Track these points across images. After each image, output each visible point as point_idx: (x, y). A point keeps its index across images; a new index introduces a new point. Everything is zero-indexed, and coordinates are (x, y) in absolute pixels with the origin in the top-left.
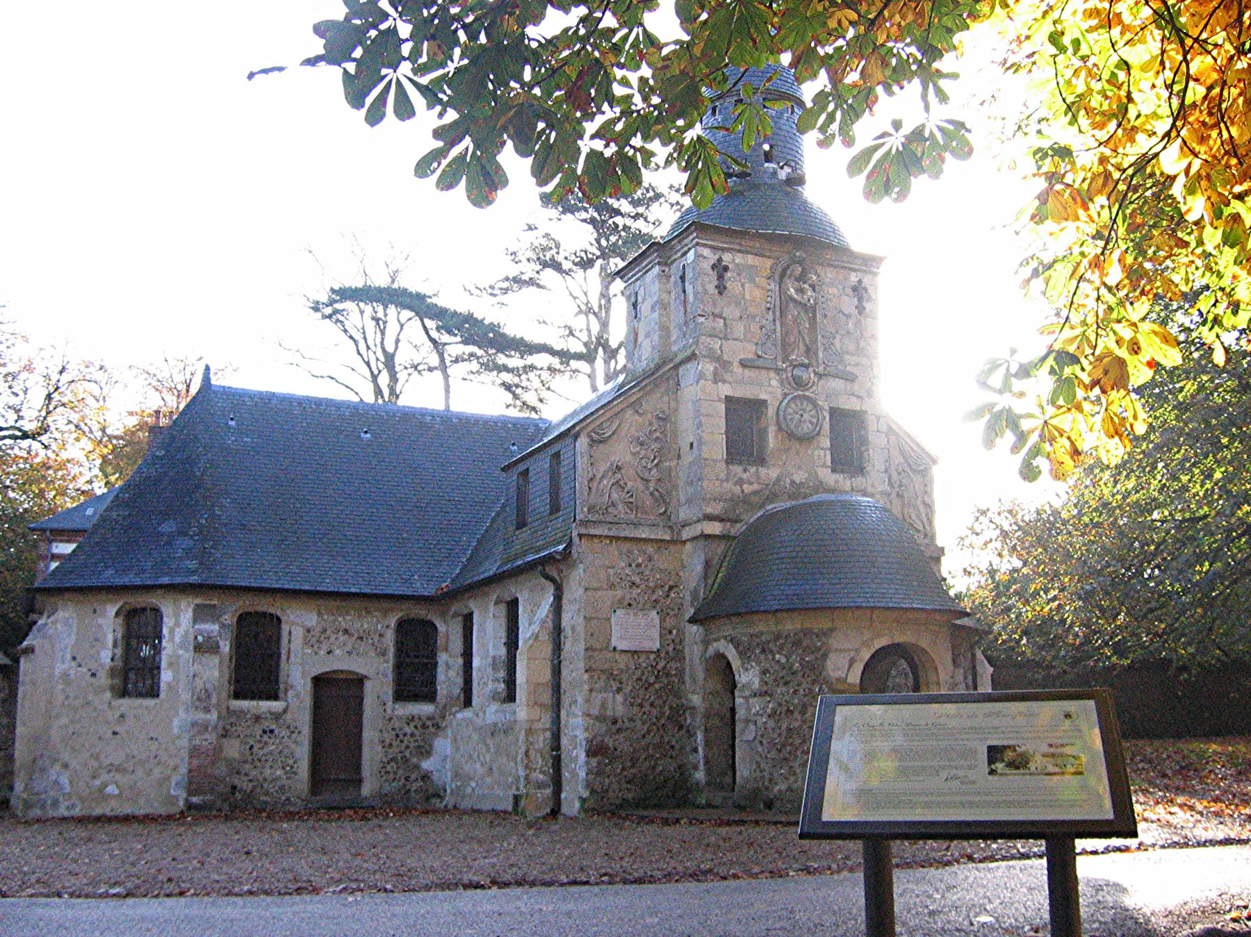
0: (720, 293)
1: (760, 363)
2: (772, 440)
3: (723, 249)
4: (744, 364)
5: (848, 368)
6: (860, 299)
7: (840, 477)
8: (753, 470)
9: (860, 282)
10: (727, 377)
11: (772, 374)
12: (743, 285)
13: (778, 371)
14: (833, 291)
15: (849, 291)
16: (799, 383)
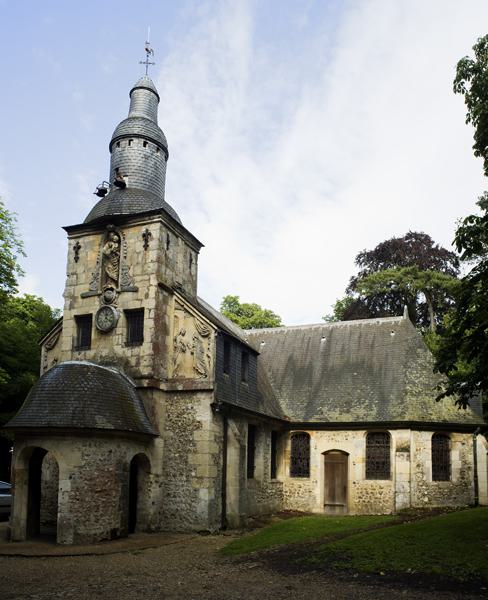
2: (93, 336)
4: (84, 297)
5: (136, 285)
6: (146, 241)
7: (125, 349)
8: (83, 353)
9: (147, 230)
10: (76, 306)
11: (96, 298)
13: (99, 295)
14: (132, 241)
15: (141, 238)
16: (108, 301)
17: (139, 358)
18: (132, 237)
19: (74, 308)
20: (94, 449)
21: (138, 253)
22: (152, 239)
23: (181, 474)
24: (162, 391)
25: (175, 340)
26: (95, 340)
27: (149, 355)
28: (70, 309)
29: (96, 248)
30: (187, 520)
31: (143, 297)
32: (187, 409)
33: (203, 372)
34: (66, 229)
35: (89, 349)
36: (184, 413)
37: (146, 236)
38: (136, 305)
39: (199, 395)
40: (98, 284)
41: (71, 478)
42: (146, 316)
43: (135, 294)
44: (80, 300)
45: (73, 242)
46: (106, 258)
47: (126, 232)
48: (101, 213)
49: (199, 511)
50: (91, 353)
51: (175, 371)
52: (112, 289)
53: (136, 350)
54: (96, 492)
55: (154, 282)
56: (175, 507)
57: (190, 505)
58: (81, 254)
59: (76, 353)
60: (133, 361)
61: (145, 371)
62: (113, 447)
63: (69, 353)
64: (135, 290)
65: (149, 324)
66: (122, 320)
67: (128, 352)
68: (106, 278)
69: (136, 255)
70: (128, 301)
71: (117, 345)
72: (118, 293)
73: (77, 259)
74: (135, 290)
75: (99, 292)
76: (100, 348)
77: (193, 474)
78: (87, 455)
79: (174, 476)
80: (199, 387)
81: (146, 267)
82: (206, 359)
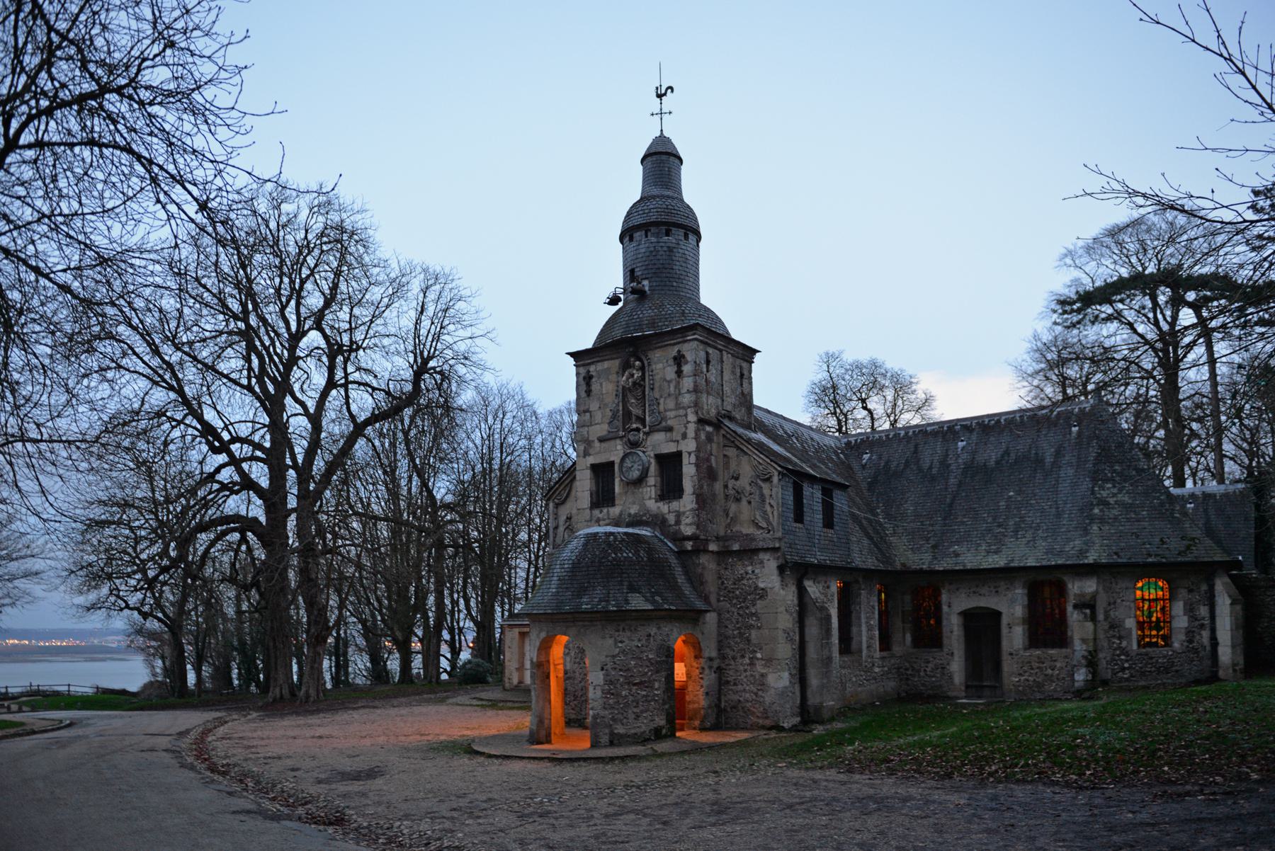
0: (589, 395)
1: (611, 435)
2: (617, 488)
3: (589, 364)
4: (601, 440)
7: (660, 504)
8: (605, 510)
9: (679, 351)
11: (618, 441)
12: (601, 384)
13: (621, 438)
14: (660, 366)
15: (671, 362)
17: (679, 515)
18: (661, 364)
19: (590, 455)
20: (628, 634)
21: (669, 382)
22: (687, 362)
23: (743, 657)
24: (712, 552)
25: (726, 486)
26: (620, 494)
27: (692, 510)
28: (584, 457)
29: (613, 377)
30: (753, 713)
31: (679, 438)
32: (747, 573)
33: (765, 525)
34: (572, 354)
35: (613, 505)
36: (743, 578)
37: (679, 360)
38: (670, 448)
39: (762, 556)
40: (620, 424)
41: (602, 669)
42: (685, 460)
43: (669, 434)
44: (597, 444)
45: (582, 370)
46: (624, 393)
47: (650, 355)
48: (618, 333)
49: (768, 700)
50: (615, 511)
51: (728, 526)
52: (638, 430)
53: (675, 505)
54: (635, 684)
55: (692, 418)
56: (736, 697)
57: (756, 694)
58: (595, 387)
59: (596, 512)
60: (671, 519)
61: (688, 531)
62: (653, 631)
63: (588, 511)
64: (669, 429)
65: (689, 470)
66: (653, 468)
67: (664, 508)
68: (627, 415)
69: (666, 384)
70: (660, 443)
71: (649, 499)
72: (647, 434)
73: (589, 392)
74: (669, 429)
75: (621, 433)
76: (625, 504)
77: (759, 655)
78: (621, 642)
79: (734, 658)
80: (761, 544)
81: (680, 399)
82: (768, 508)
